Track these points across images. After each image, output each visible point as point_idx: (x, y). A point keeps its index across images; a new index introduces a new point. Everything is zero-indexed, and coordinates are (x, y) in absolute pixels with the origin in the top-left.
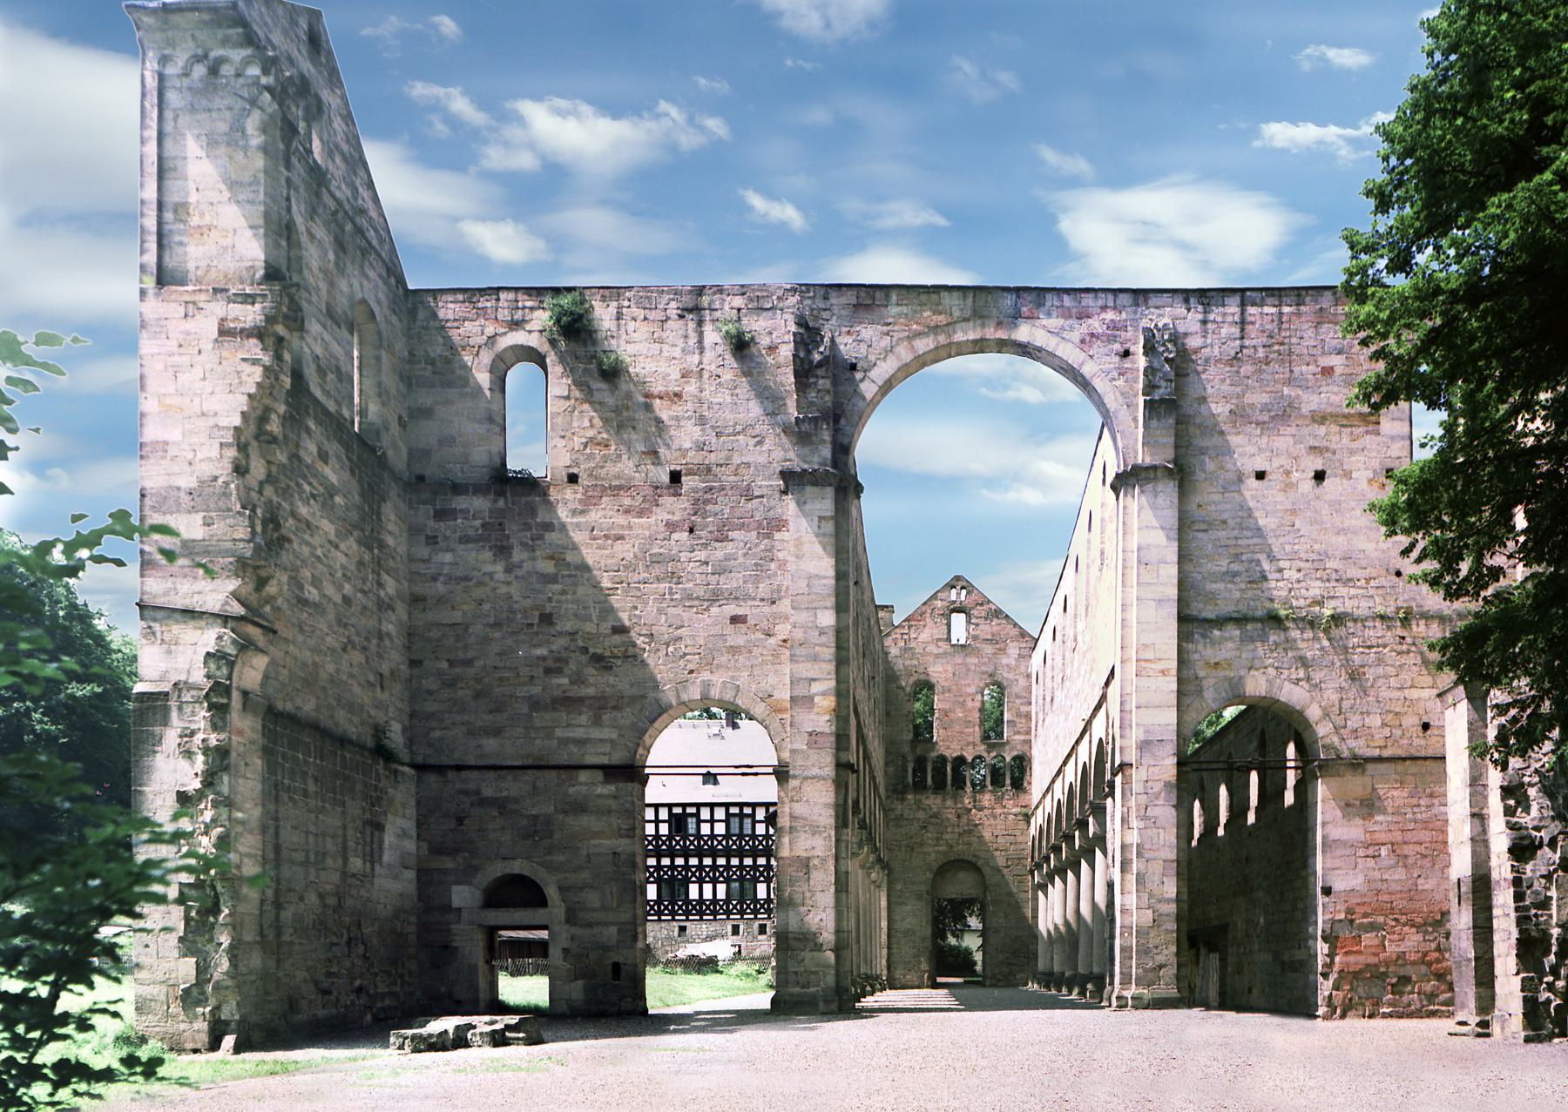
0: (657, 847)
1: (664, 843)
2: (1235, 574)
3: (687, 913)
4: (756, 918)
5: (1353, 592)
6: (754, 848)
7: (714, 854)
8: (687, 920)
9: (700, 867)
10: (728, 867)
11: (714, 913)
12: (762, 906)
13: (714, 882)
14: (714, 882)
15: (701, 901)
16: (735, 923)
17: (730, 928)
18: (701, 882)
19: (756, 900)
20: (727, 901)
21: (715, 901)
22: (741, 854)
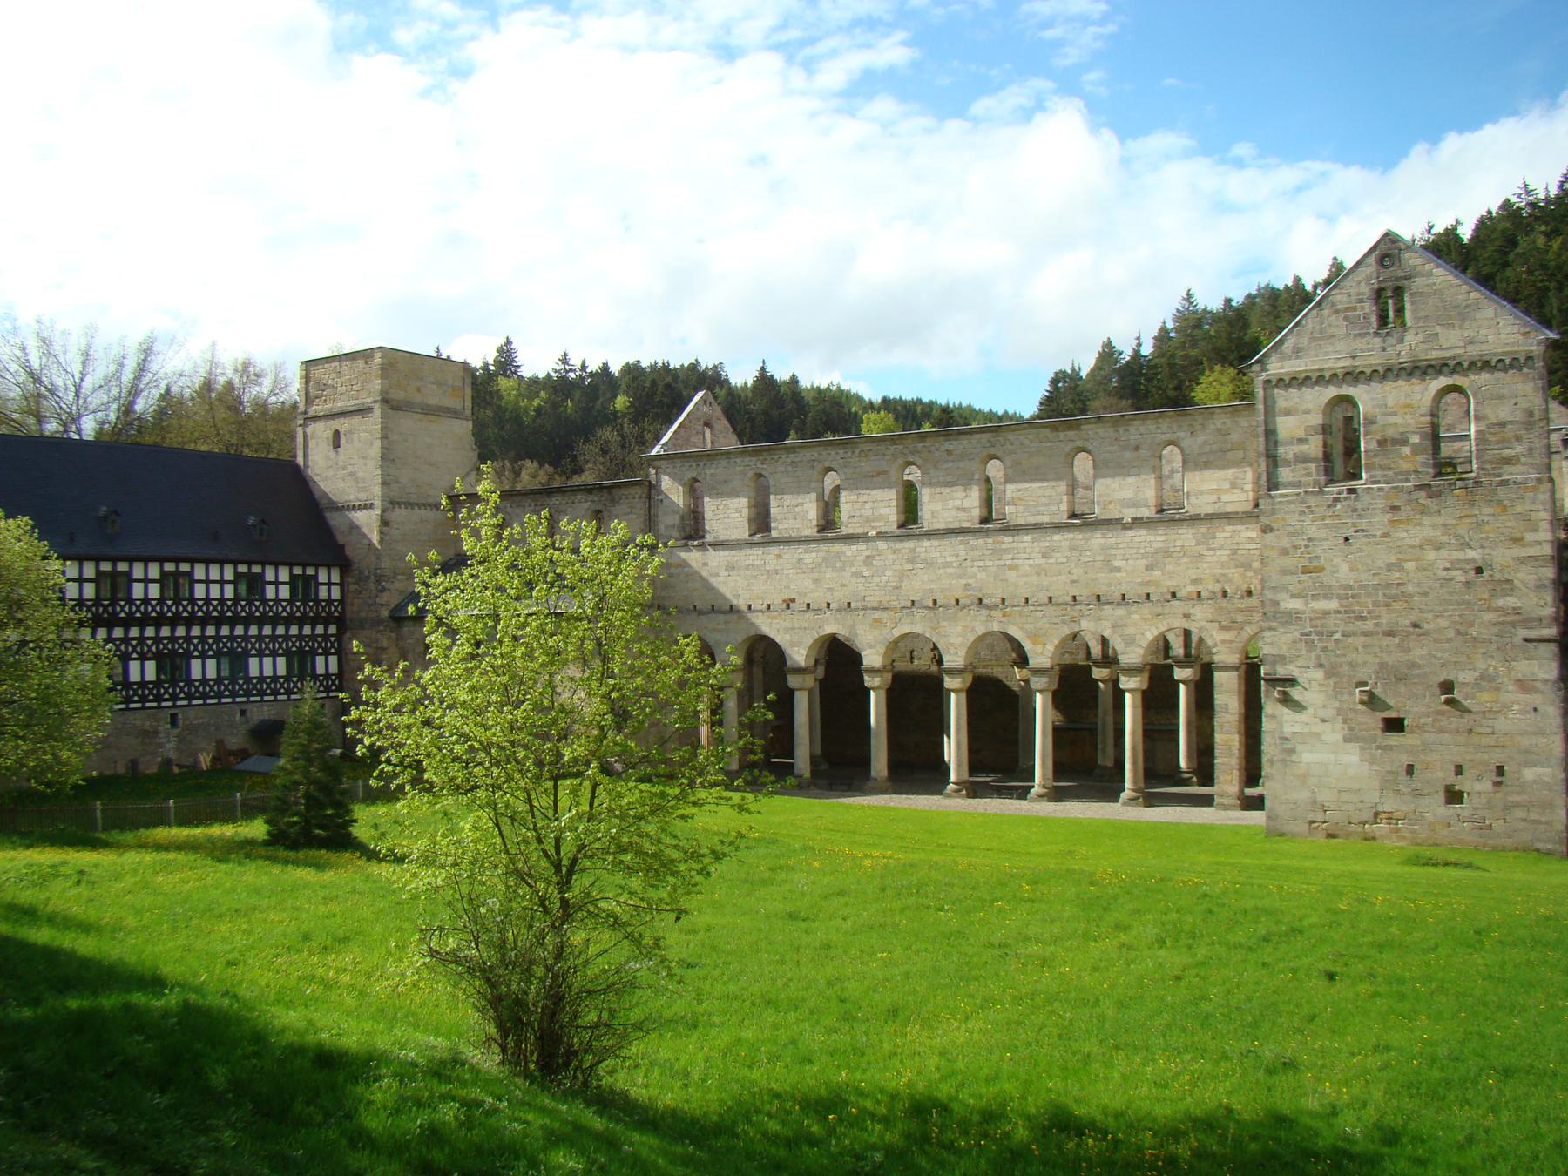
0: (222, 613)
1: (229, 609)
3: (248, 694)
6: (317, 614)
7: (275, 621)
8: (248, 702)
9: (260, 637)
10: (287, 637)
11: (275, 692)
13: (274, 654)
15: (261, 678)
18: (261, 655)
20: (288, 678)
21: (275, 678)
22: (301, 623)
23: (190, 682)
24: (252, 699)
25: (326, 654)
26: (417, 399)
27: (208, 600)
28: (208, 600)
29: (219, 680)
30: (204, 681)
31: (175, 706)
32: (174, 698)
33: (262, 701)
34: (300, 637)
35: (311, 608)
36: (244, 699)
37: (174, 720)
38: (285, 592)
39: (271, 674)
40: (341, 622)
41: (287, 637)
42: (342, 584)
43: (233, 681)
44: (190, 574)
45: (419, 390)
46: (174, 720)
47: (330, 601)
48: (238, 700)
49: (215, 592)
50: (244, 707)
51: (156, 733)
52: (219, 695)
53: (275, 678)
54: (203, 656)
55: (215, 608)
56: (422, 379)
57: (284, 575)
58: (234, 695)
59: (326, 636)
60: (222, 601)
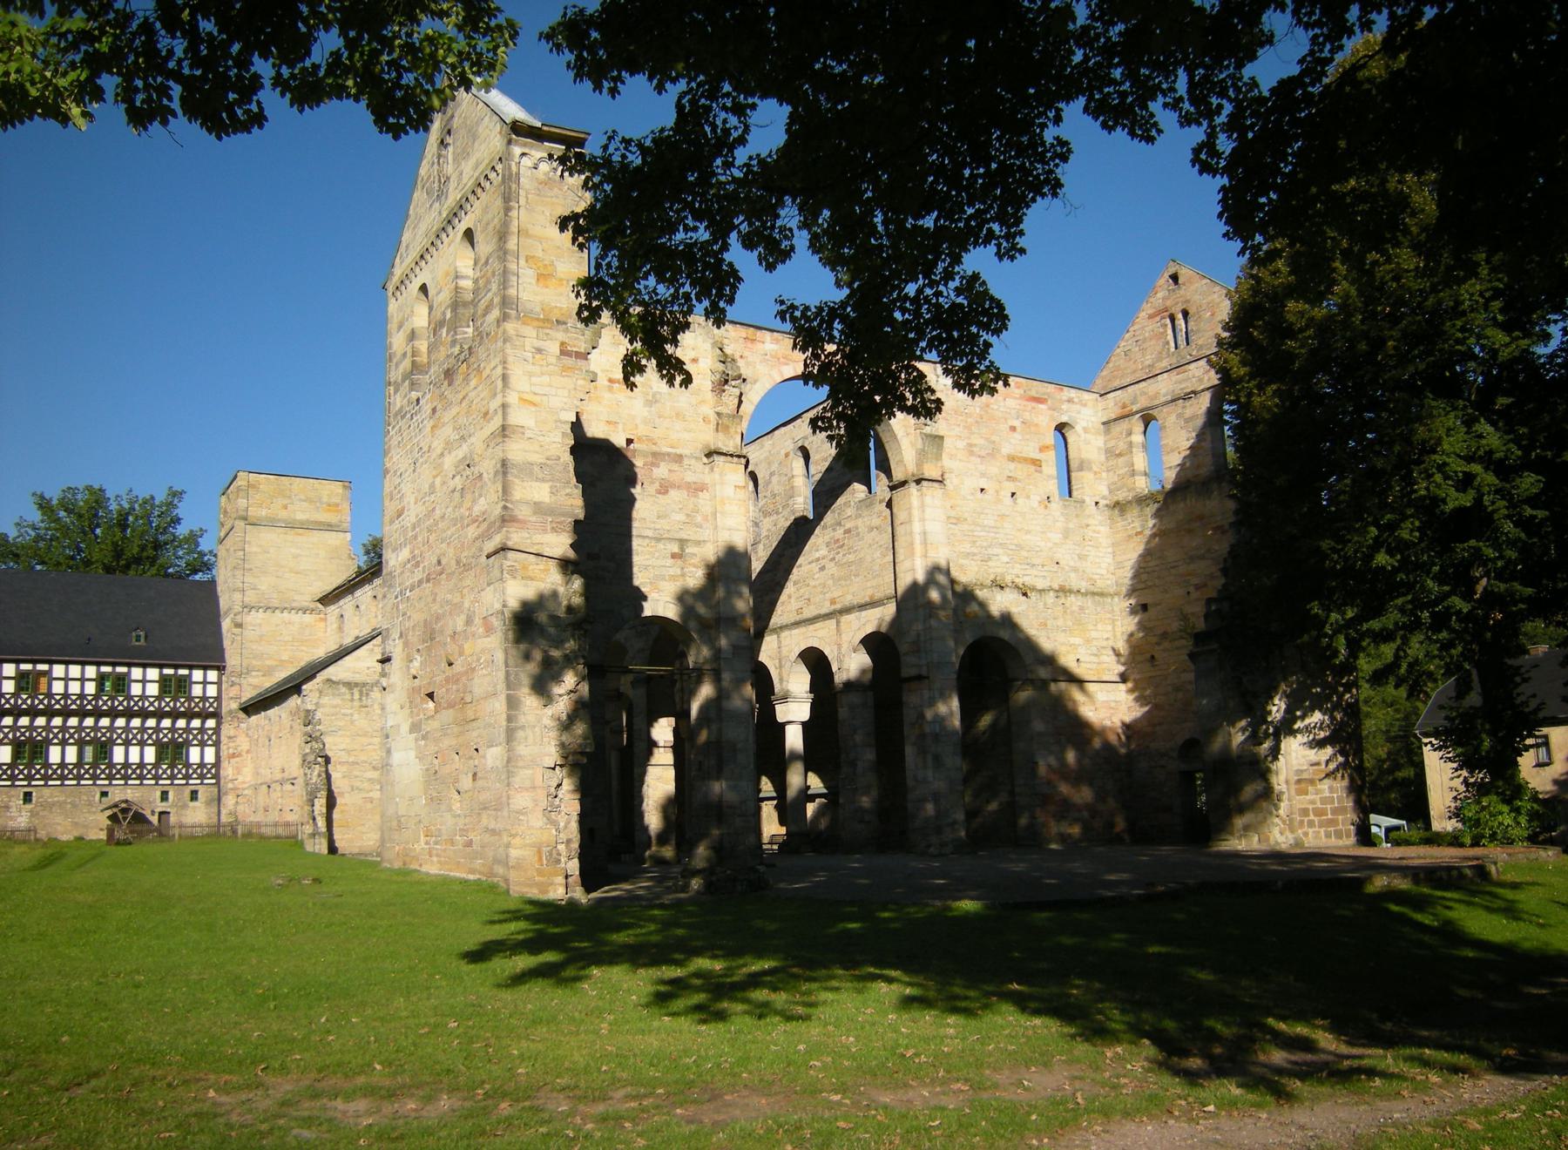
2: (974, 554)
3: (110, 777)
4: (187, 784)
5: (1035, 572)
7: (144, 715)
8: (110, 784)
11: (141, 777)
12: (195, 772)
13: (142, 744)
14: (142, 744)
15: (126, 765)
16: (165, 788)
17: (158, 794)
18: (127, 743)
19: (188, 765)
20: (156, 765)
21: (142, 765)
23: (47, 765)
24: (114, 782)
25: (202, 744)
26: (283, 514)
27: (66, 696)
28: (66, 696)
29: (80, 763)
30: (63, 765)
31: (29, 785)
32: (30, 778)
33: (126, 784)
34: (173, 729)
35: (182, 704)
36: (107, 782)
37: (28, 797)
38: (153, 690)
39: (138, 761)
40: (216, 715)
41: (157, 729)
42: (219, 683)
43: (95, 765)
44: (48, 673)
45: (285, 507)
46: (28, 797)
47: (204, 698)
48: (99, 782)
49: (74, 688)
50: (105, 789)
51: (7, 807)
52: (79, 777)
53: (142, 765)
54: (64, 743)
55: (74, 702)
56: (290, 497)
57: (153, 673)
58: (95, 777)
59: (202, 730)
60: (82, 696)
